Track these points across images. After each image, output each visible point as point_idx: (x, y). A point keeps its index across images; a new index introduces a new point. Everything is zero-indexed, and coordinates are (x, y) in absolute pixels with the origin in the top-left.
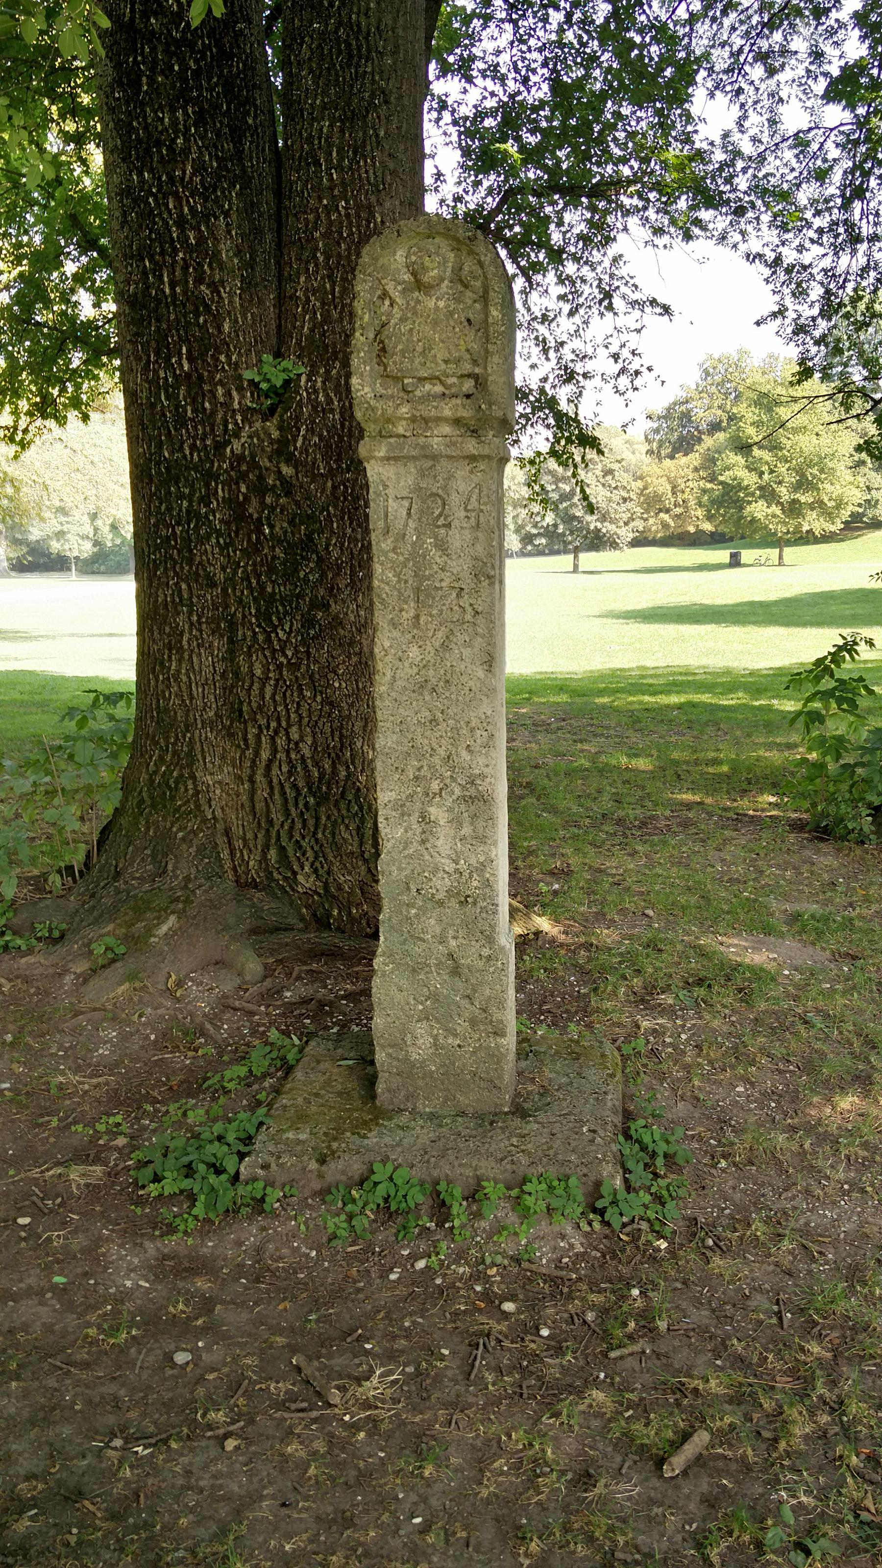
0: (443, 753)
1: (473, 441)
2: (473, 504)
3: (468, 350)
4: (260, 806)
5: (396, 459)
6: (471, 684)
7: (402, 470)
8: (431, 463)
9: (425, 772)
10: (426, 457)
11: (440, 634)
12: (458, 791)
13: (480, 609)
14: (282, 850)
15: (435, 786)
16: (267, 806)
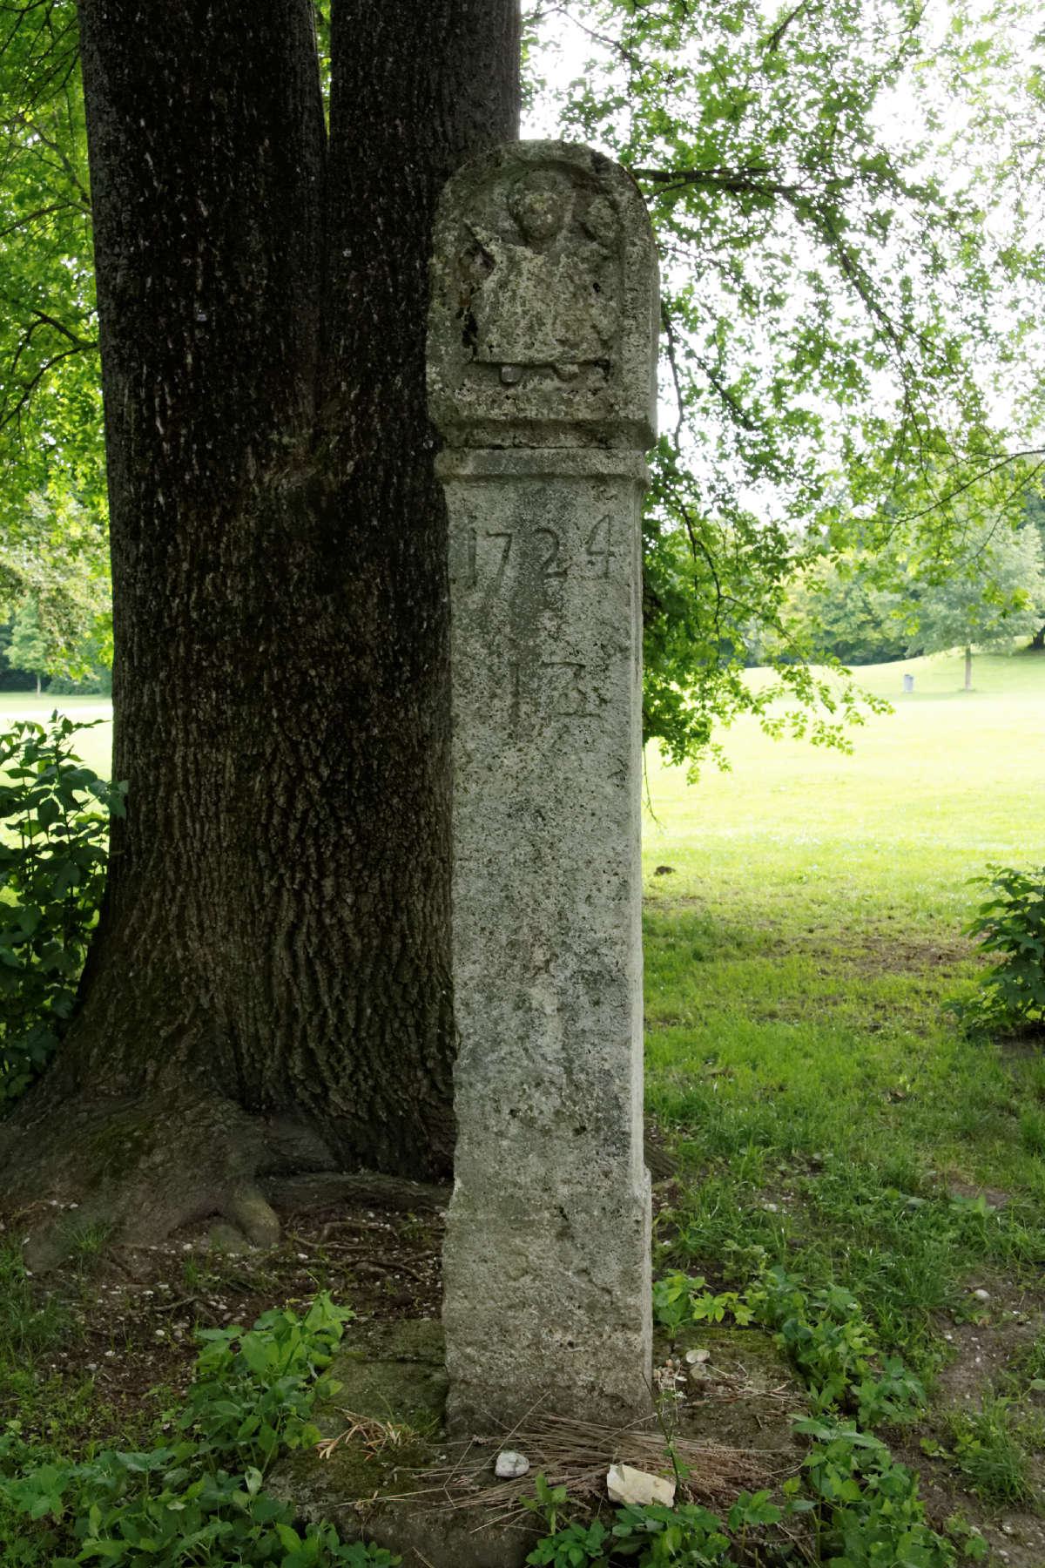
0: (552, 909)
4: (279, 991)
6: (595, 805)
9: (525, 934)
11: (547, 732)
12: (573, 964)
13: (608, 696)
14: (309, 1055)
15: (539, 956)
16: (290, 992)
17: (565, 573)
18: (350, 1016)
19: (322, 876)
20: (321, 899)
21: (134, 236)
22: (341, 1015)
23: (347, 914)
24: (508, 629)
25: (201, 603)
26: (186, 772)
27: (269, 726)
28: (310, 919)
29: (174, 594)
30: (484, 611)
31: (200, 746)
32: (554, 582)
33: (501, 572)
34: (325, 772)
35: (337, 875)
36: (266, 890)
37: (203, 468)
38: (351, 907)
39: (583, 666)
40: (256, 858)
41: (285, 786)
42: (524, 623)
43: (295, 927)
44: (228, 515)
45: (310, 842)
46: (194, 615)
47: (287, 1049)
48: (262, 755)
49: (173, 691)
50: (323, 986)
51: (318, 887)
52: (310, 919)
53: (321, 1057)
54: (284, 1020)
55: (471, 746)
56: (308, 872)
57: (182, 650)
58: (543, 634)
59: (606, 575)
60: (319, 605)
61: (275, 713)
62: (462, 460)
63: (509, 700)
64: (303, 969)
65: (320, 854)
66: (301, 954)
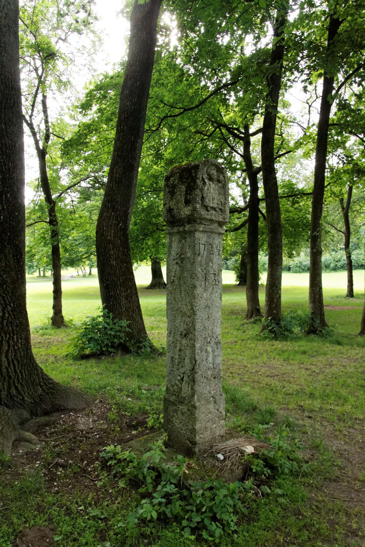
14: (16, 388)
16: (7, 370)
18: (24, 374)
19: (14, 335)
20: (14, 341)
22: (22, 374)
28: (12, 348)
35: (17, 334)
43: (8, 351)
47: (9, 388)
50: (17, 367)
51: (13, 338)
52: (12, 348)
53: (20, 388)
54: (7, 379)
56: (10, 334)
64: (11, 363)
66: (10, 359)
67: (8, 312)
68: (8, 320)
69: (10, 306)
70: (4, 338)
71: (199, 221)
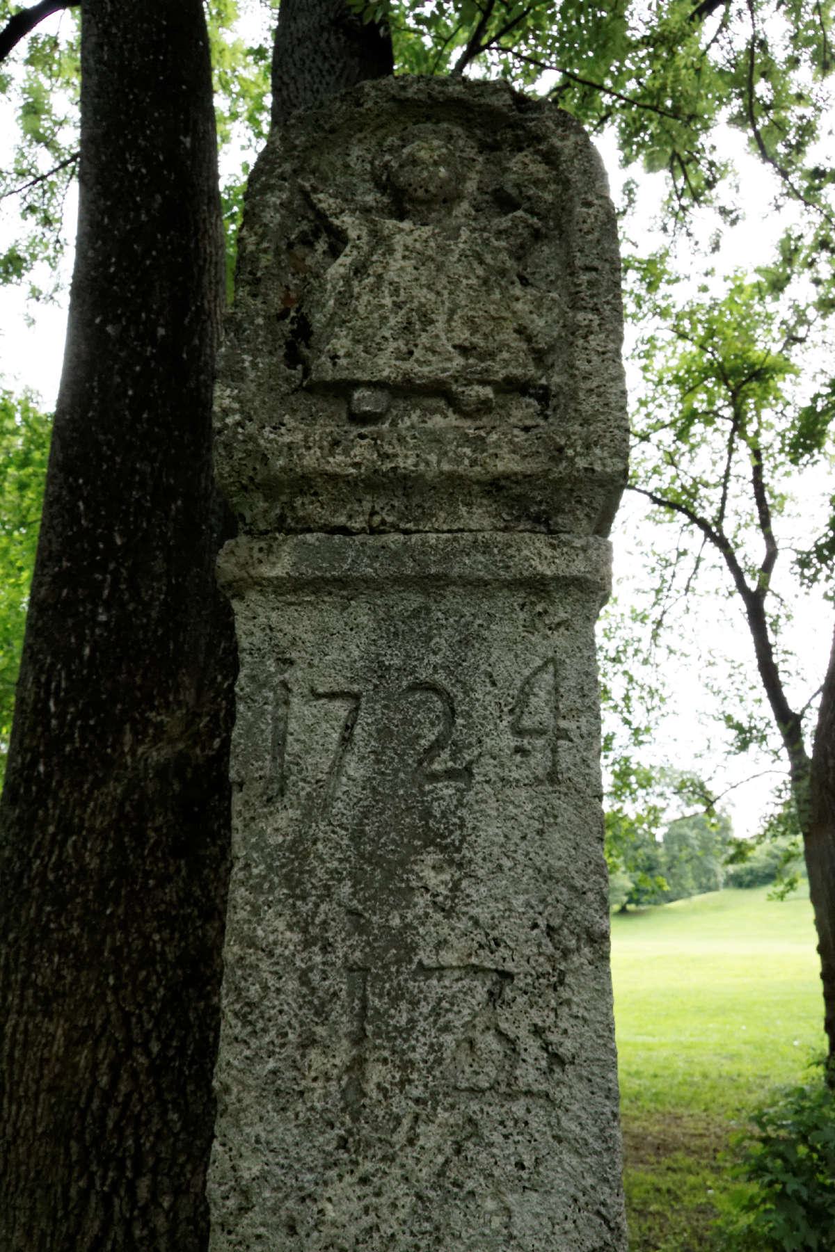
1: (540, 542)
2: (539, 709)
3: (520, 330)
5: (317, 586)
7: (333, 619)
8: (415, 600)
10: (401, 581)
11: (430, 1136)
13: (568, 1047)
17: (468, 772)
19: (138, 1174)
21: (60, 561)
23: (161, 1223)
24: (346, 889)
25: (60, 864)
26: (14, 1044)
27: (104, 995)
28: (118, 1232)
29: (36, 856)
30: (299, 848)
31: (32, 1014)
32: (446, 790)
33: (337, 769)
34: (155, 1048)
35: (154, 1171)
36: (73, 1192)
37: (83, 741)
38: (167, 1213)
39: (506, 976)
40: (68, 1149)
41: (111, 1066)
42: (380, 872)
44: (98, 783)
45: (129, 1131)
46: (51, 877)
48: (91, 1026)
49: (17, 954)
51: (132, 1189)
52: (118, 1232)
55: (251, 1168)
56: (121, 1168)
57: (32, 912)
58: (422, 900)
59: (553, 777)
60: (172, 869)
61: (111, 981)
62: (270, 551)
63: (343, 1053)
65: (139, 1146)
67: (134, 1075)
68: (126, 1104)
69: (148, 1053)
70: (98, 1183)
71: (257, 508)
